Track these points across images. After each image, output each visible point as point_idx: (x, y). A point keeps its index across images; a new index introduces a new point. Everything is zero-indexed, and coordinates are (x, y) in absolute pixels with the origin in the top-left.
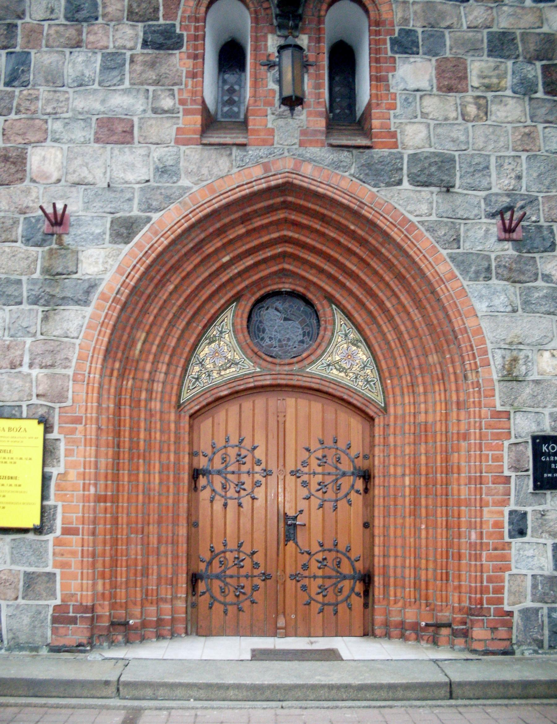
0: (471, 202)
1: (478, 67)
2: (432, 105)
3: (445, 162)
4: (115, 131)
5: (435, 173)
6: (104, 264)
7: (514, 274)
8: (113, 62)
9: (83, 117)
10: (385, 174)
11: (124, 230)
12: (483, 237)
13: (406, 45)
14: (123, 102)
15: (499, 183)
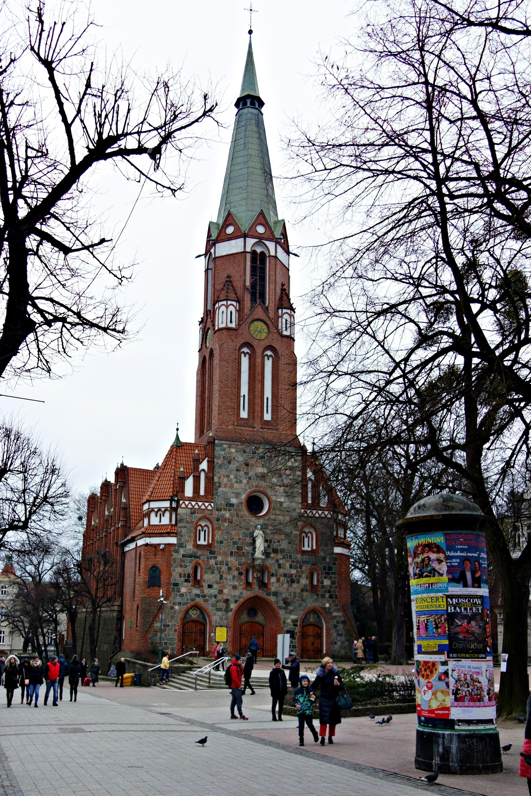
0: (280, 598)
1: (282, 579)
2: (275, 584)
3: (277, 592)
4: (235, 587)
5: (276, 594)
6: (233, 606)
7: (285, 608)
8: (234, 577)
9: (231, 585)
10: (269, 594)
11: (236, 601)
12: (281, 604)
13: (273, 575)
14: (236, 583)
15: (284, 596)
